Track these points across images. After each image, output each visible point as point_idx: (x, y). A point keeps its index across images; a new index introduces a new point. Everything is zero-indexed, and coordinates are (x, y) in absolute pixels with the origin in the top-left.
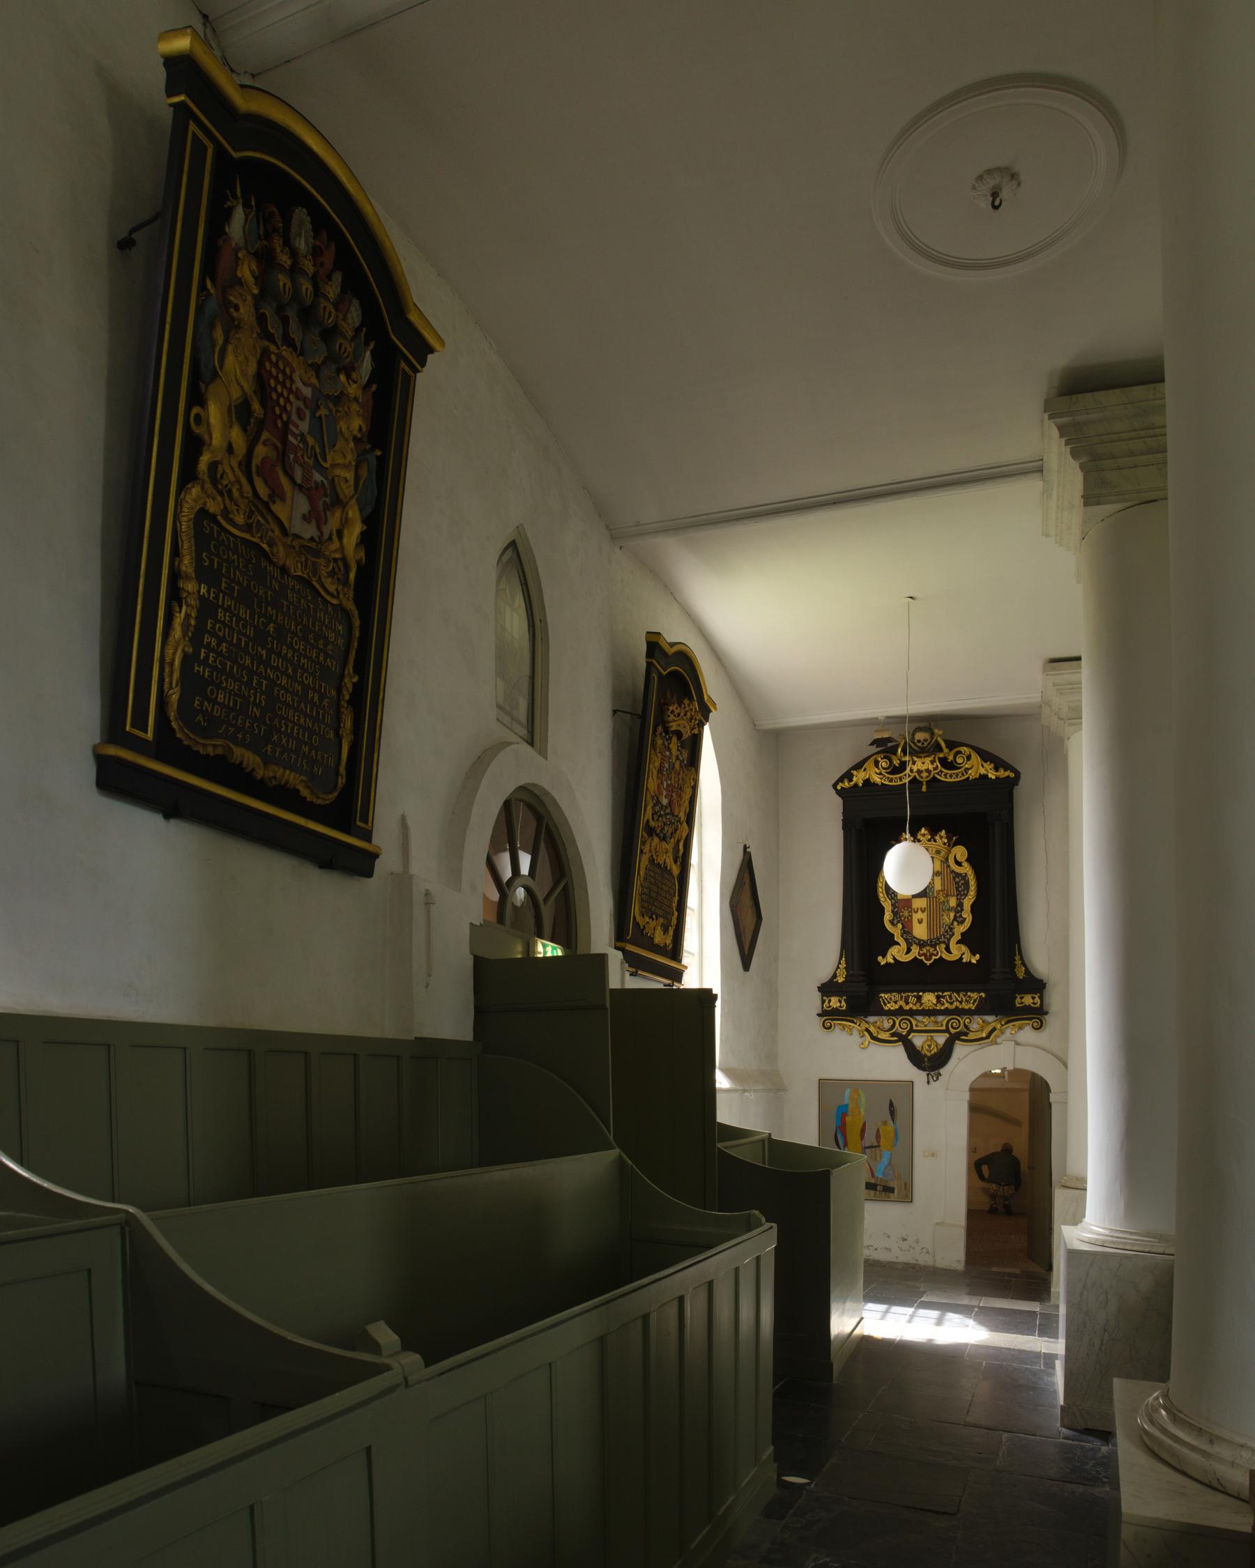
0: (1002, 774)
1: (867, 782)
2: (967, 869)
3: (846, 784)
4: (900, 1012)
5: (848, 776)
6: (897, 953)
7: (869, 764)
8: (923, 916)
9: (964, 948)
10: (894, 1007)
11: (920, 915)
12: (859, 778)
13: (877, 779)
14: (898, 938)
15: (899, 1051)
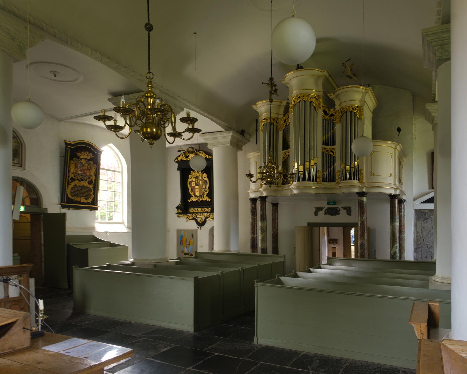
0: (210, 157)
1: (181, 160)
2: (207, 179)
3: (177, 160)
4: (194, 213)
5: (177, 158)
6: (193, 199)
7: (181, 156)
8: (198, 190)
9: (207, 197)
10: (192, 211)
11: (198, 190)
12: (180, 159)
13: (183, 159)
14: (193, 195)
15: (194, 222)
